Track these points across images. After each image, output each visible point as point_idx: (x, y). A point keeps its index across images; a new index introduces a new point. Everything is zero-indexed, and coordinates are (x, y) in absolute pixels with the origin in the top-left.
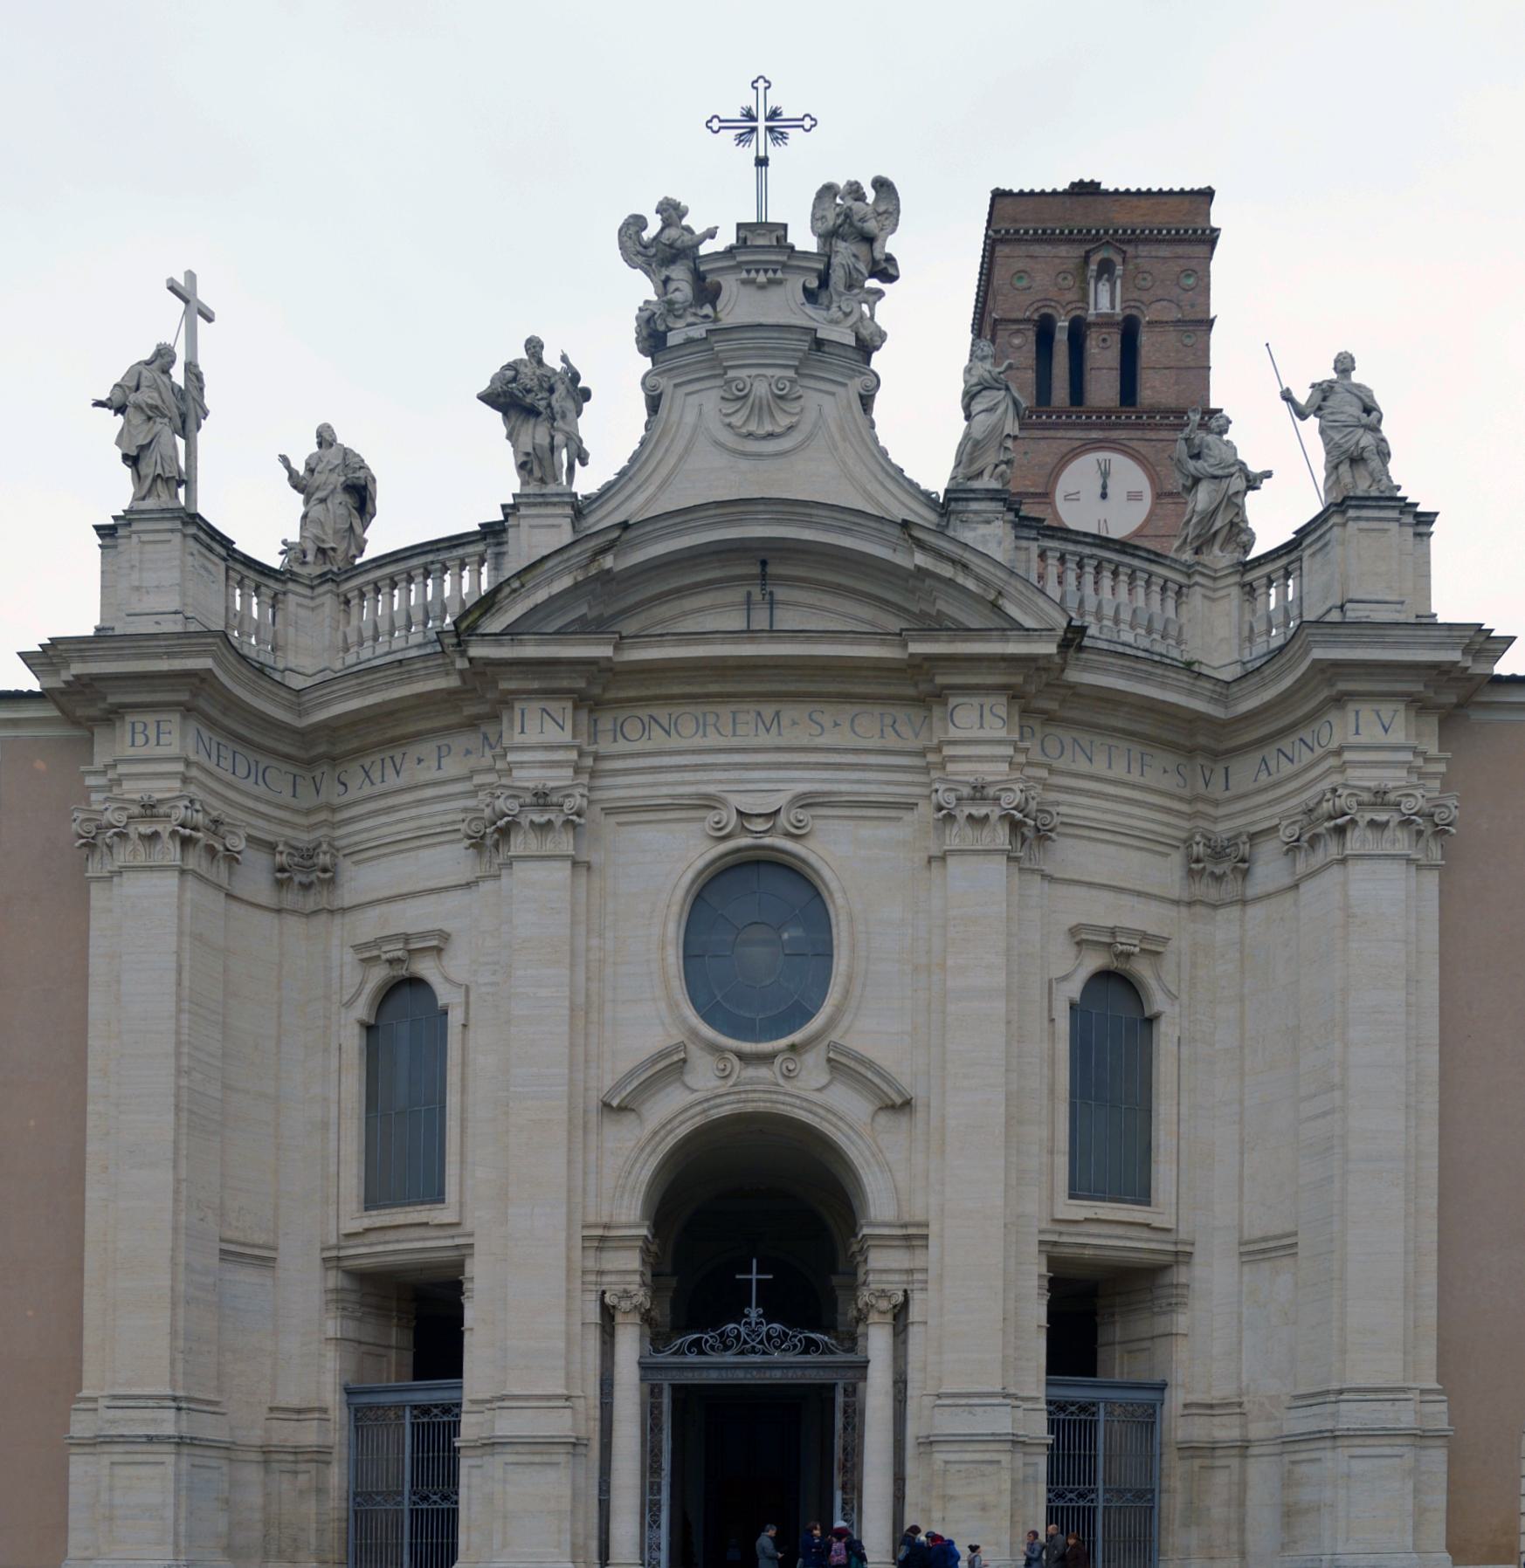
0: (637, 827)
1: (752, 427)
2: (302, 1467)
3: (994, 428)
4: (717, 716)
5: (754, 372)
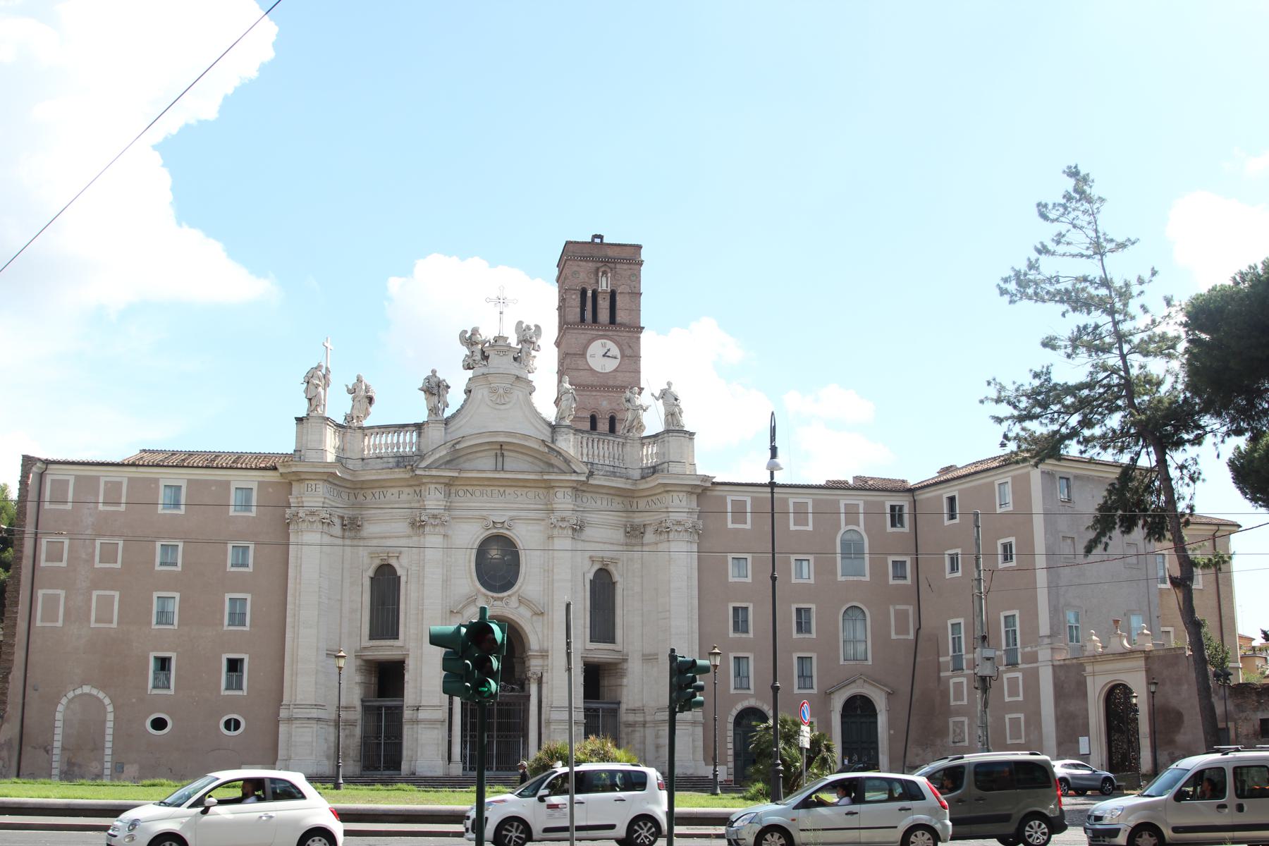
2: (347, 727)
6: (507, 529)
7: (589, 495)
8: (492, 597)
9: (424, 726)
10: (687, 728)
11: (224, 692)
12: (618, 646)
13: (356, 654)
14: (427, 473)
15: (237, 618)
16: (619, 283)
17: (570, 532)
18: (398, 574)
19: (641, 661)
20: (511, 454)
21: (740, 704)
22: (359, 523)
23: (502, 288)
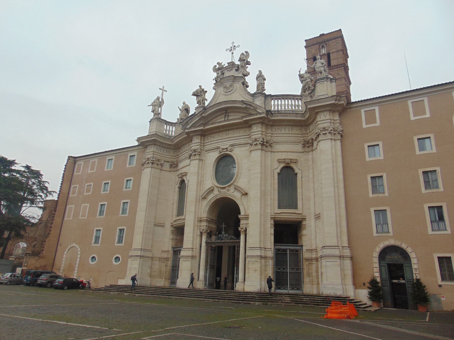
0: (210, 153)
1: (227, 91)
2: (165, 261)
3: (260, 83)
4: (220, 134)
5: (227, 83)
6: (229, 151)
7: (276, 128)
8: (220, 188)
9: (183, 259)
10: (336, 260)
11: (116, 245)
12: (299, 211)
13: (171, 224)
14: (189, 130)
15: (124, 211)
16: (330, 49)
17: (260, 147)
18: (186, 183)
19: (314, 219)
20: (232, 114)
21: (382, 243)
22: (175, 163)
23: (233, 43)
